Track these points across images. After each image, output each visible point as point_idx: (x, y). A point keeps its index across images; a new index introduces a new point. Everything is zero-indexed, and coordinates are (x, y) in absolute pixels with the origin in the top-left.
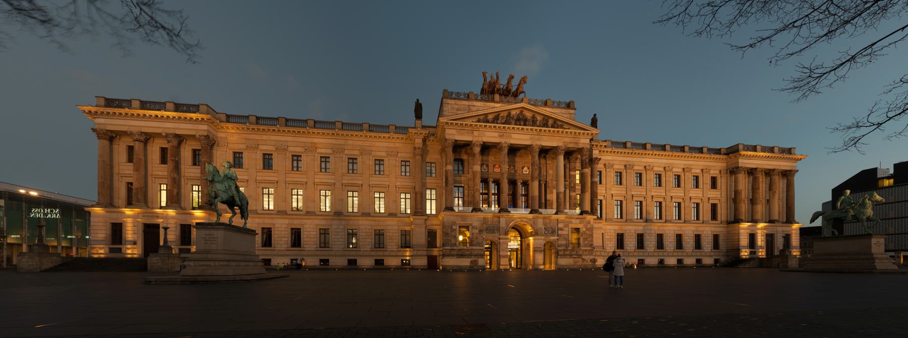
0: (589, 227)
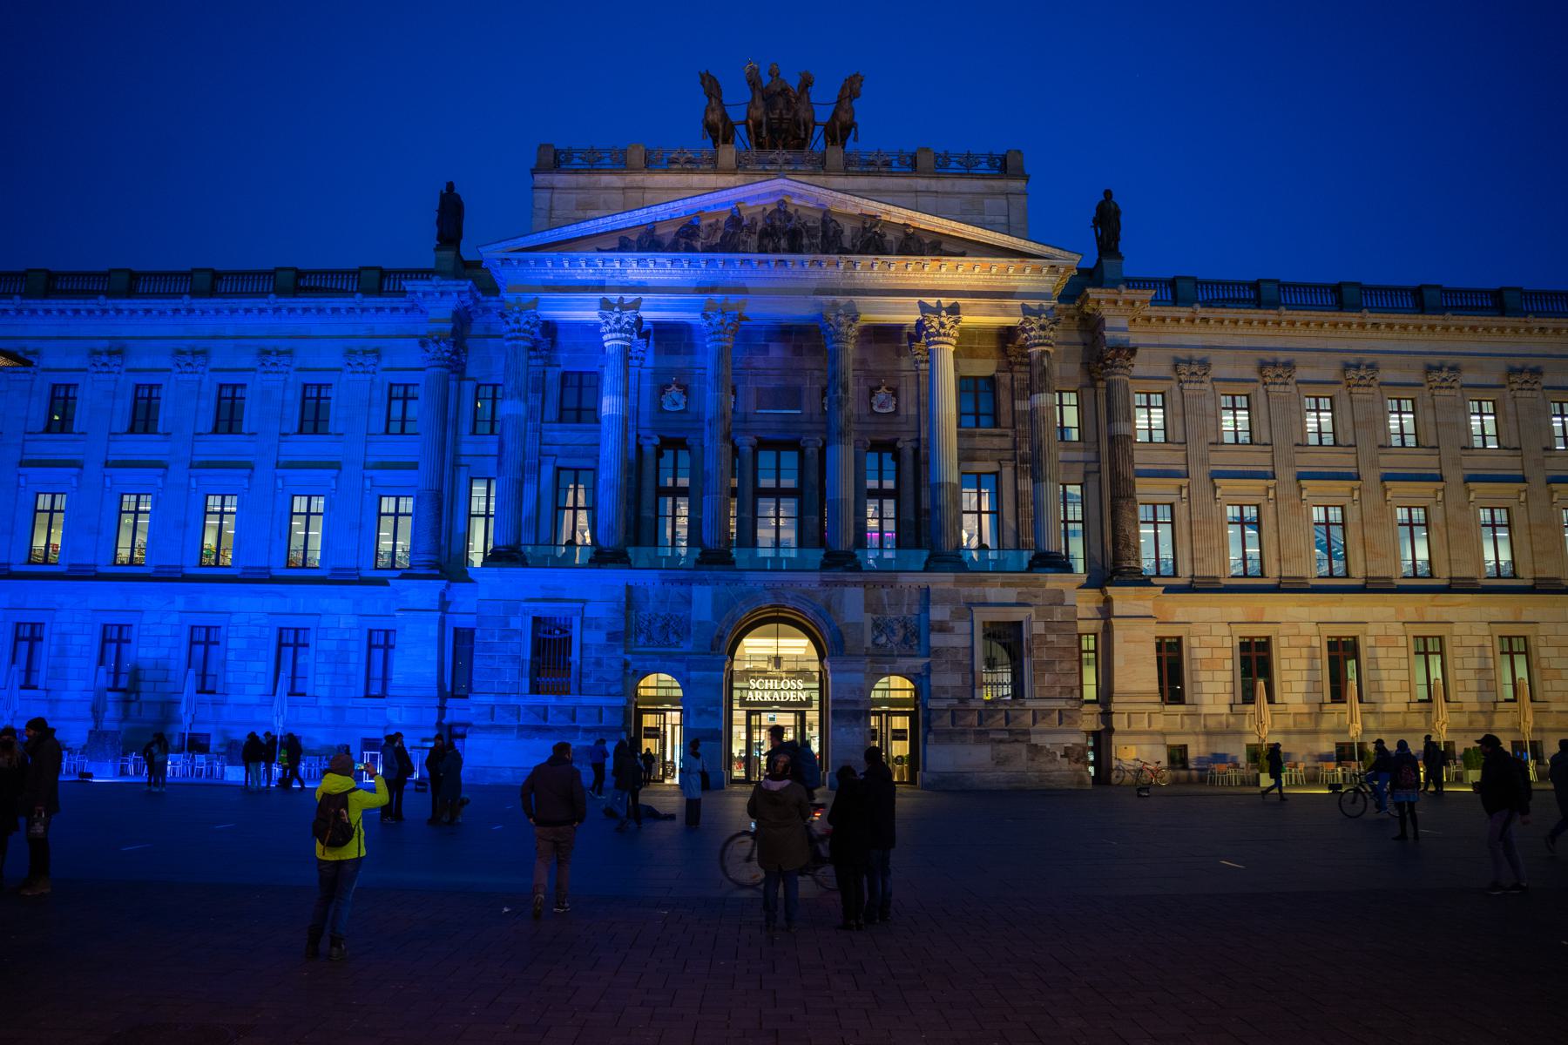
0: (1058, 617)
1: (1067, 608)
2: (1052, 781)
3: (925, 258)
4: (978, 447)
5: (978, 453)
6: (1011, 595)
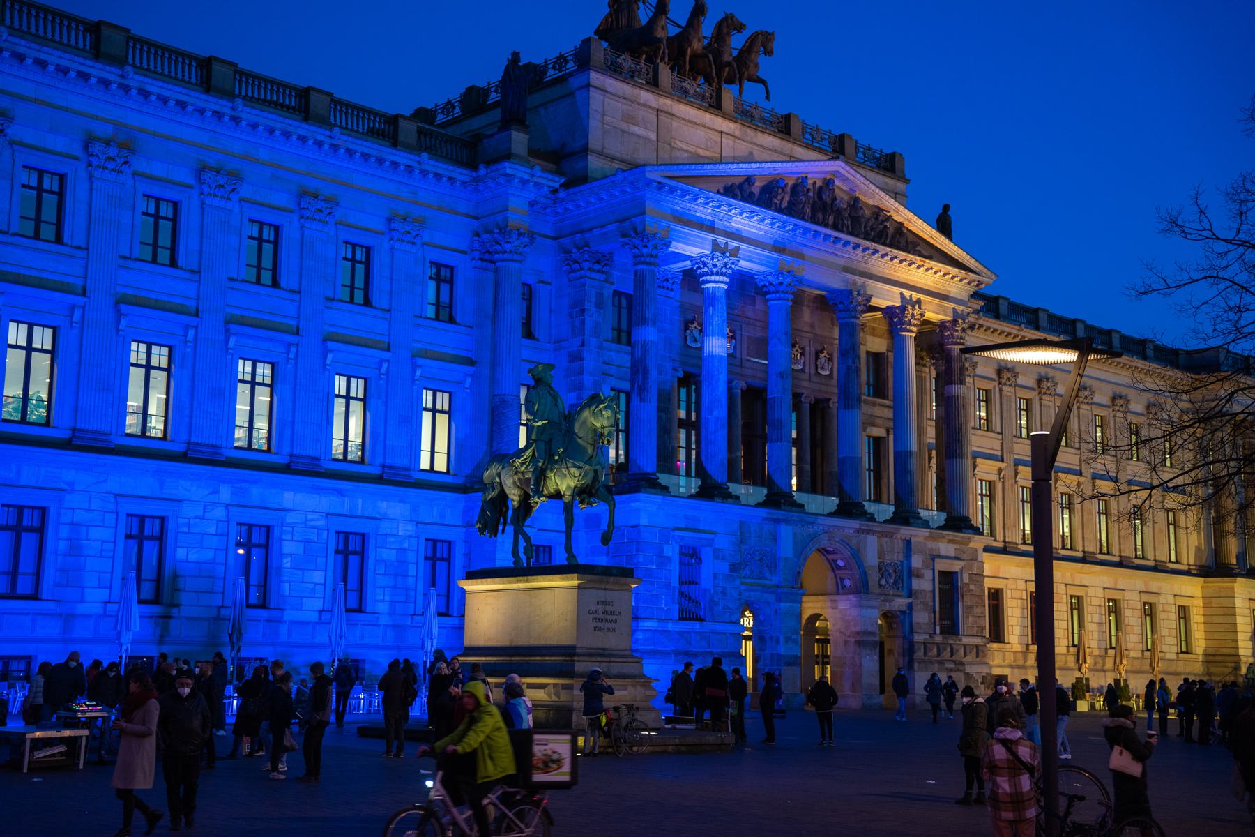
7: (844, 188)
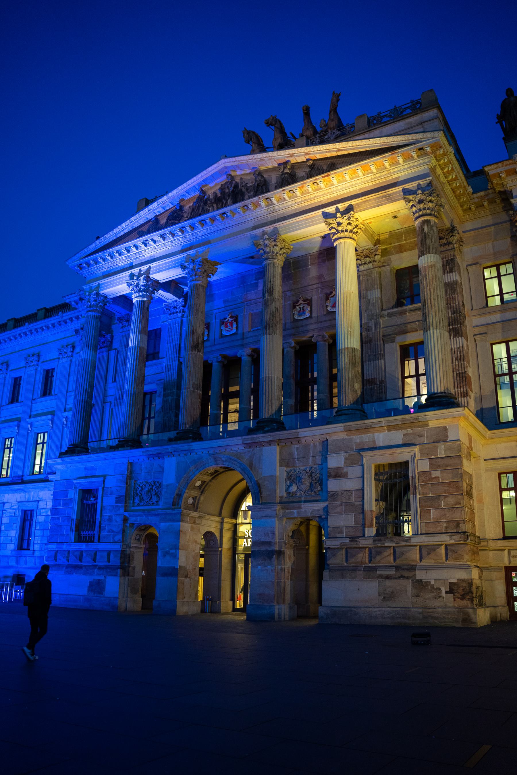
1: (451, 443)
2: (436, 618)
3: (318, 177)
4: (409, 321)
5: (409, 326)
6: (398, 437)
7: (248, 172)
